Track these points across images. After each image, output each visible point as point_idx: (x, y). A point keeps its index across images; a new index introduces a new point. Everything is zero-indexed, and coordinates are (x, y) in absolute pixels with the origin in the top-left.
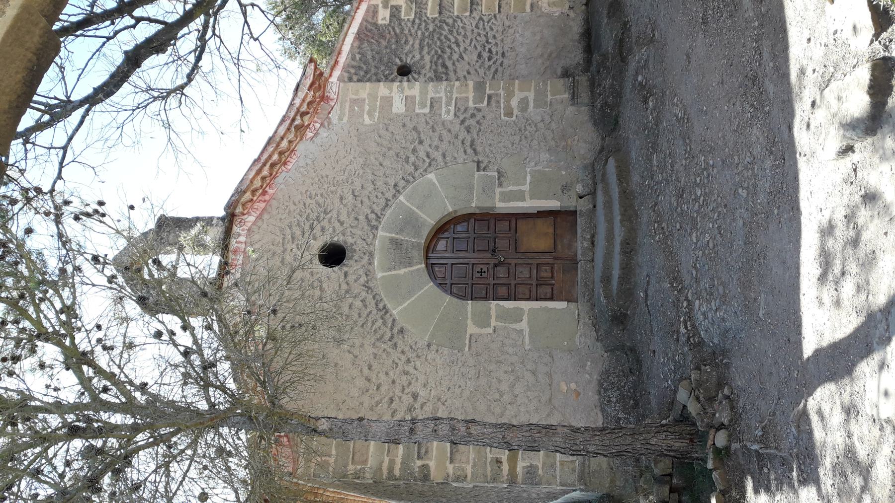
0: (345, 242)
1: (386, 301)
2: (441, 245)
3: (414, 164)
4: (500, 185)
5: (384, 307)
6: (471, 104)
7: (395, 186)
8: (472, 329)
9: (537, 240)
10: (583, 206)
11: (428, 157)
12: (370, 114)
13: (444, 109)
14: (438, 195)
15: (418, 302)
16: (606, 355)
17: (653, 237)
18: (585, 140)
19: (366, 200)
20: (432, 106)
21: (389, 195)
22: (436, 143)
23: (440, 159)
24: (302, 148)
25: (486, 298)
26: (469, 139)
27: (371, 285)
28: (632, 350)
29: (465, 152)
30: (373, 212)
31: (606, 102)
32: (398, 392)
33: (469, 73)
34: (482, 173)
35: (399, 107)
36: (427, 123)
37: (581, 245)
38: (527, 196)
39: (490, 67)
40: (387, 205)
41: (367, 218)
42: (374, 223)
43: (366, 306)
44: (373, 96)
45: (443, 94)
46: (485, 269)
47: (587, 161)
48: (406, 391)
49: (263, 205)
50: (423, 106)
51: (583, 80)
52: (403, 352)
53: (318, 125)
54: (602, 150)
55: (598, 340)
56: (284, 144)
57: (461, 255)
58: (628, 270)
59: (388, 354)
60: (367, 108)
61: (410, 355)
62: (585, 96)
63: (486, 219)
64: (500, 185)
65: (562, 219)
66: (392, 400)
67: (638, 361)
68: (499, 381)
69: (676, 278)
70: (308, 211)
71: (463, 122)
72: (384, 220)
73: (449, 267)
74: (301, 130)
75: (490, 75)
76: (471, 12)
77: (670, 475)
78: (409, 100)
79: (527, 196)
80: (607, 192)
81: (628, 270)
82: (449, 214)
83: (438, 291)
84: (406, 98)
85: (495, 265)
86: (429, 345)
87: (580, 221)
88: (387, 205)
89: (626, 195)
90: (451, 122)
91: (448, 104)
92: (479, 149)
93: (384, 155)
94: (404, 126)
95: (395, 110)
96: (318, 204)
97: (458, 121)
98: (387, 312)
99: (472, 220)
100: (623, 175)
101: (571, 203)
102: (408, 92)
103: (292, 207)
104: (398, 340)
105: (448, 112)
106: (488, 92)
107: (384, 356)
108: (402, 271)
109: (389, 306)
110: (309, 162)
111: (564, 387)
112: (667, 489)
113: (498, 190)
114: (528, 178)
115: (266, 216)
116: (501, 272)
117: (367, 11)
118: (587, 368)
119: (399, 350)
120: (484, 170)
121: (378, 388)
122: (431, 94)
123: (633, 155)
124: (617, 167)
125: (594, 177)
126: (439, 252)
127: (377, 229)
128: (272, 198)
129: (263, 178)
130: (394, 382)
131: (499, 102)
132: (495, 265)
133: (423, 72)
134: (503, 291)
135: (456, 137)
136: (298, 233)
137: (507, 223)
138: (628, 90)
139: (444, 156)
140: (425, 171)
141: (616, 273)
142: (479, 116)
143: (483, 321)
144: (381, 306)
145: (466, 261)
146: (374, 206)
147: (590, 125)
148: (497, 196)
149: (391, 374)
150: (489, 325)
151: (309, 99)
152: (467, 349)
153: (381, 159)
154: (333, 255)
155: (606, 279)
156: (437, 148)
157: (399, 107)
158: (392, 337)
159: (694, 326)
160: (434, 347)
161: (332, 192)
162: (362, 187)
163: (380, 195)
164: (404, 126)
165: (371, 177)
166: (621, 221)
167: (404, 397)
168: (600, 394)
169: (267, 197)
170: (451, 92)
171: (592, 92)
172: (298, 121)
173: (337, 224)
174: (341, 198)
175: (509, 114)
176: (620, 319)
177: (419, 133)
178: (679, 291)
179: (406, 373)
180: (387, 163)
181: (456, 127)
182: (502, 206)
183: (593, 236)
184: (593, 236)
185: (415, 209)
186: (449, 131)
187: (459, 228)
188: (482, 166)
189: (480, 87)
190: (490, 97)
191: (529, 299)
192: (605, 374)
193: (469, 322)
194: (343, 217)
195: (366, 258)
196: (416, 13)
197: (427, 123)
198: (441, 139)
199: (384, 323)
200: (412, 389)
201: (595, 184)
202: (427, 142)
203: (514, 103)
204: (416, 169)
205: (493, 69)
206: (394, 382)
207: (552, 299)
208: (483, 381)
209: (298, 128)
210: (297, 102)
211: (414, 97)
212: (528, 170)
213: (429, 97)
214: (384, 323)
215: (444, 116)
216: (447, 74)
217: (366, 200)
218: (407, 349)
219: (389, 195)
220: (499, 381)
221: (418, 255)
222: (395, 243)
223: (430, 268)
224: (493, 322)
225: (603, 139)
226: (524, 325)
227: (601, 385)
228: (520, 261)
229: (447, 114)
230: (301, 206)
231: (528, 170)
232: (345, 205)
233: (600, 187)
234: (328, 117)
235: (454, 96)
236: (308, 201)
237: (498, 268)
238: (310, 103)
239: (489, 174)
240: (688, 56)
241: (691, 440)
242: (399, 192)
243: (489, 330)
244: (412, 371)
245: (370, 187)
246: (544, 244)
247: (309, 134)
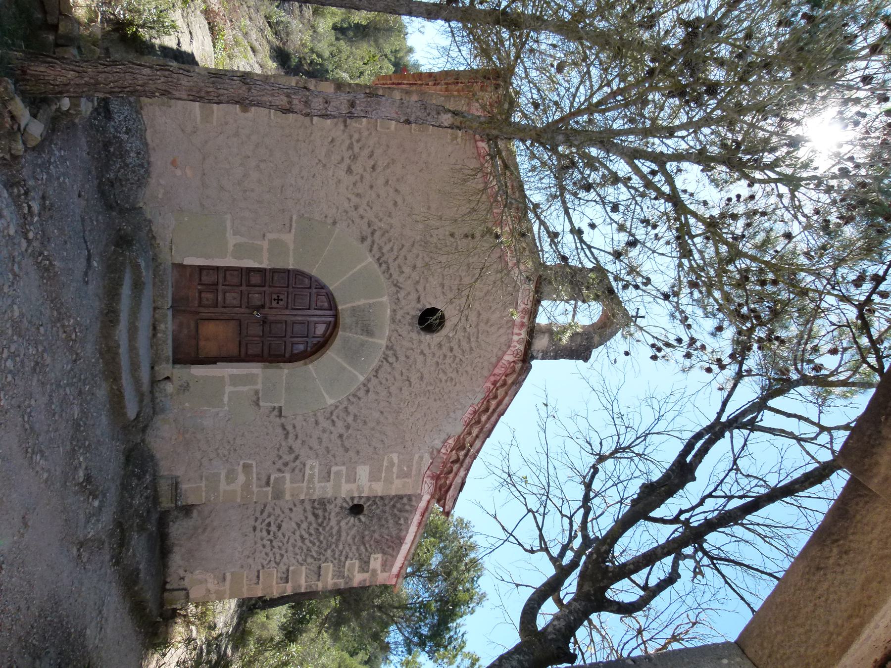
0: (418, 333)
1: (379, 271)
2: (320, 329)
3: (348, 413)
4: (257, 392)
5: (380, 265)
6: (288, 476)
7: (368, 391)
8: (288, 238)
9: (216, 334)
10: (165, 369)
11: (333, 421)
12: (392, 464)
13: (316, 470)
14: (323, 382)
15: (345, 270)
16: (141, 205)
17: (78, 324)
18: (163, 440)
19: (398, 376)
20: (329, 473)
21: (374, 381)
22: (326, 435)
23: (321, 419)
24: (457, 428)
25: (274, 271)
26: (291, 440)
27: (394, 289)
28: (110, 207)
29: (294, 427)
30: (391, 364)
31: (139, 479)
32: (367, 176)
33: (291, 510)
34: (276, 405)
35: (363, 472)
36: (334, 456)
37: (168, 326)
38: (227, 380)
39: (269, 516)
40: (377, 371)
41: (397, 358)
42: (390, 353)
43: (400, 267)
44: (389, 481)
45: (317, 485)
46: (274, 303)
47: (161, 417)
48: (358, 177)
49: (497, 371)
50: (338, 473)
51: (166, 503)
52: (362, 217)
53: (443, 451)
54: (144, 430)
55: (150, 221)
56: (475, 431)
57: (300, 319)
58: (112, 293)
59: (377, 217)
60: (395, 470)
61: (354, 214)
62: (164, 487)
63: (273, 356)
64: (257, 392)
65: (189, 355)
66: (373, 167)
67: (103, 194)
68: (259, 181)
69: (46, 271)
70: (454, 365)
71: (297, 458)
72: (380, 355)
73: (313, 305)
74: (460, 446)
75: (268, 509)
76: (288, 570)
77: (57, 45)
79: (227, 380)
80: (137, 382)
81: (112, 293)
82: (311, 362)
83: (325, 280)
85: (263, 306)
86: (334, 223)
87: (168, 351)
88: (377, 371)
89: (112, 375)
90: (308, 457)
91: (312, 476)
92: (279, 430)
93: (378, 423)
94: (358, 452)
95: (366, 469)
96: (444, 372)
97: (301, 459)
98: (378, 259)
99: (287, 355)
100: (117, 400)
101: (181, 373)
102: (353, 486)
103: (469, 369)
104: (367, 231)
105: (312, 468)
106: (269, 489)
107: (381, 214)
108: (362, 302)
109: (376, 266)
110: (452, 414)
111: (189, 172)
112: (62, 29)
113: (259, 386)
114: (226, 399)
115: (494, 360)
116: (256, 299)
117: (392, 566)
118: (162, 191)
119: (366, 220)
120: (274, 408)
121: (387, 182)
122: (330, 485)
123: (104, 420)
124: (123, 407)
125: (153, 400)
126: (324, 322)
127: (387, 347)
128: (487, 378)
129: (495, 397)
130: (371, 187)
131: (258, 479)
132: (263, 306)
133: (337, 509)
134: (255, 279)
136: (464, 344)
137: (250, 352)
139: (317, 423)
140: (337, 407)
141: (126, 291)
142: (279, 464)
143: (276, 244)
144: (384, 266)
145: (295, 312)
146: (389, 370)
147: (158, 456)
148: (260, 381)
149: (374, 196)
150: (270, 241)
151: (451, 476)
152: (295, 217)
153: (382, 419)
154: (430, 320)
155: (138, 286)
156: (324, 431)
157: (363, 472)
158: (373, 234)
159: (19, 207)
160: (330, 221)
161: (431, 384)
162: (401, 389)
163: (384, 381)
164: (358, 452)
165: (393, 400)
166: (118, 346)
167: (361, 171)
168: (149, 163)
169: (492, 379)
170: (309, 488)
171: (156, 490)
172: (462, 454)
173: (426, 351)
174: (422, 378)
175: (246, 467)
176: (123, 241)
177: (343, 445)
178: (41, 254)
179: (358, 195)
180: (376, 415)
181: (303, 452)
182: (255, 369)
183: (154, 335)
184: (154, 335)
185: (350, 368)
186: (311, 448)
187: (301, 347)
188: (276, 412)
189: (278, 495)
190: (268, 484)
191: (227, 269)
192: (142, 182)
193: (292, 247)
194: (420, 359)
195: (398, 317)
196: (344, 566)
197: (334, 456)
199: (380, 248)
200: (353, 179)
201: (152, 392)
202: (334, 437)
203: (241, 478)
204: (346, 408)
205: (265, 514)
206: (371, 187)
207: (201, 268)
209: (462, 447)
210: (462, 473)
211: (348, 481)
212: (226, 408)
213: (332, 482)
214: (380, 248)
215: (316, 463)
216: (314, 508)
217: (398, 376)
218: (357, 220)
219: (374, 381)
220: (259, 181)
221: (345, 319)
222: (368, 331)
223: (332, 305)
224: (265, 245)
225: (143, 441)
226: (232, 240)
227: (148, 172)
228: (236, 310)
229: (313, 466)
230: (460, 370)
231: (226, 408)
232: (419, 371)
233: (146, 387)
234: (433, 459)
235: (305, 484)
236: (454, 375)
237: (259, 303)
238: (450, 472)
239: (268, 404)
240: (26, 525)
241: (24, 72)
242: (364, 385)
243: (270, 236)
244: (353, 197)
245: (393, 389)
246: (210, 329)
247: (451, 441)
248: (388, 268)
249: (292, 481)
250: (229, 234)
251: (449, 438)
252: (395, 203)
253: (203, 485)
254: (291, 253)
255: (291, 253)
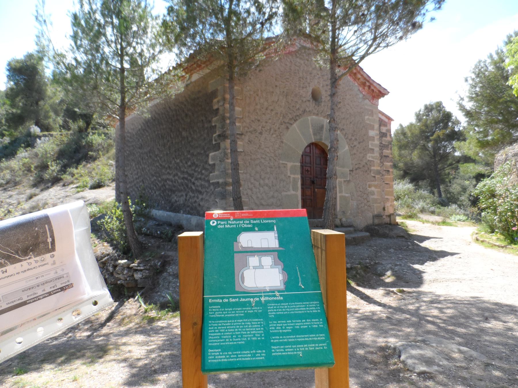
4: (345, 181)
5: (297, 120)
7: (343, 129)
8: (289, 165)
12: (368, 119)
26: (361, 166)
29: (356, 164)
38: (341, 194)
45: (375, 155)
52: (279, 128)
66: (259, 121)
68: (269, 179)
74: (364, 84)
76: (385, 171)
84: (374, 137)
91: (372, 157)
104: (283, 126)
106: (377, 176)
108: (311, 130)
109: (297, 122)
117: (385, 122)
120: (350, 173)
135: (361, 160)
138: (380, 242)
144: (297, 118)
147: (366, 224)
148: (340, 180)
150: (291, 174)
151: (375, 90)
158: (285, 123)
172: (368, 84)
188: (351, 172)
190: (374, 177)
195: (316, 112)
196: (384, 145)
198: (360, 153)
203: (373, 189)
208: (268, 170)
210: (375, 84)
213: (374, 148)
224: (292, 176)
226: (293, 192)
234: (367, 98)
238: (373, 90)
243: (289, 174)
247: (361, 89)
248: (298, 116)
249: (374, 166)
250: (289, 193)
251: (359, 90)
252: (272, 110)
253: (375, 205)
254: (295, 164)
255: (295, 164)
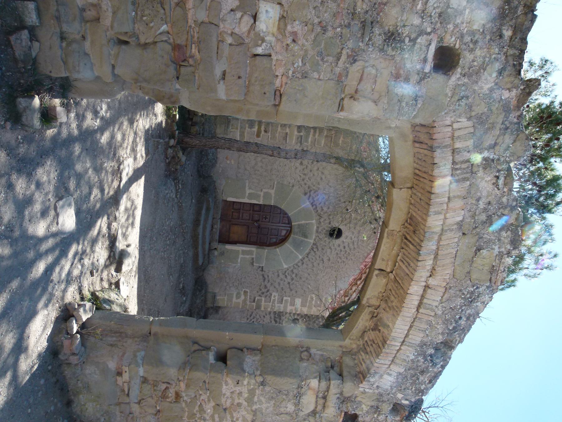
0: (329, 238)
1: (312, 208)
2: (284, 233)
3: (293, 273)
4: (253, 259)
5: (313, 206)
6: (263, 299)
7: (303, 263)
8: (272, 192)
9: (238, 231)
10: (215, 245)
11: (286, 276)
13: (276, 298)
14: (283, 258)
16: (212, 175)
17: (187, 226)
18: (211, 275)
19: (318, 258)
20: (282, 300)
21: (306, 259)
22: (282, 282)
23: (281, 274)
24: (347, 286)
25: (265, 205)
26: (266, 282)
27: (318, 217)
28: (200, 176)
30: (315, 252)
31: (200, 291)
32: (309, 166)
33: (264, 316)
34: (261, 265)
35: (298, 301)
36: (285, 292)
37: (218, 226)
38: (241, 252)
39: (254, 318)
40: (308, 255)
41: (318, 249)
42: (315, 246)
43: (322, 207)
44: (310, 307)
45: (277, 305)
46: (264, 219)
47: (211, 265)
48: (305, 166)
49: (367, 260)
50: (286, 301)
51: (209, 305)
52: (305, 184)
53: (338, 296)
54: (204, 270)
55: (215, 182)
56: (354, 289)
57: (274, 227)
58: (198, 213)
59: (312, 184)
60: (313, 302)
61: (302, 183)
62: (209, 296)
63: (261, 243)
64: (253, 259)
65: (225, 239)
67: (198, 171)
68: (262, 167)
69: (180, 207)
70: (345, 255)
71: (268, 291)
72: (310, 247)
73: (281, 222)
75: (254, 315)
77: (192, 125)
78: (293, 304)
79: (241, 252)
80: (204, 249)
81: (198, 213)
82: (278, 247)
83: (288, 212)
85: (259, 220)
86: (293, 186)
87: (217, 237)
88: (308, 255)
89: (195, 247)
90: (273, 291)
91: (274, 300)
92: (261, 277)
93: (307, 279)
94: (296, 292)
95: (300, 300)
96: (340, 258)
97: (270, 292)
98: (312, 203)
99: (268, 243)
100: (196, 256)
101: (220, 247)
102: (293, 308)
103: (353, 258)
105: (274, 296)
106: (255, 304)
107: (314, 183)
108: (303, 222)
109: (310, 206)
110: (343, 279)
111: (233, 162)
112: (194, 120)
113: (254, 256)
114: (239, 261)
115: (366, 255)
116: (256, 217)
118: (221, 169)
119: (307, 185)
121: (318, 169)
122: (282, 306)
123: (190, 264)
124: (198, 260)
125: (209, 257)
126: (285, 230)
127: (313, 244)
128: (362, 263)
129: (365, 273)
130: (311, 171)
131: (250, 298)
132: (259, 220)
133: (286, 320)
134: (256, 208)
135: (272, 284)
136: (351, 245)
137: (252, 240)
139: (278, 276)
140: (288, 269)
141: (204, 212)
142: (260, 293)
143: (267, 195)
144: (314, 207)
145: (272, 224)
146: (314, 254)
148: (255, 253)
149: (312, 175)
152: (276, 183)
153: (309, 277)
154: (336, 233)
155: (208, 209)
156: (281, 280)
157: (298, 301)
158: (310, 191)
159: (176, 187)
160: (291, 185)
161: (333, 263)
162: (319, 264)
163: (311, 260)
164: (296, 292)
165: (314, 269)
166: (199, 235)
167: (306, 164)
168: (217, 158)
169: (364, 264)
170: (272, 306)
171: (206, 298)
173: (332, 247)
174: (329, 260)
175: (245, 292)
176: (204, 190)
177: (289, 287)
178: (179, 202)
179: (304, 174)
180: (306, 275)
181: (271, 289)
182: (253, 249)
183: (212, 230)
184: (212, 230)
185: (295, 252)
186: (275, 287)
187: (274, 240)
188: (260, 269)
189: (258, 307)
190: (254, 301)
191: (244, 203)
192: (213, 165)
193: (273, 195)
194: (329, 250)
195: (320, 230)
197: (285, 292)
199: (313, 198)
200: (302, 167)
201: (208, 254)
202: (286, 283)
203: (243, 297)
204: (292, 270)
205: (252, 317)
206: (311, 171)
207: (234, 202)
209: (347, 296)
211: (291, 305)
212: (239, 264)
214: (313, 198)
215: (277, 295)
216: (275, 317)
217: (318, 258)
218: (303, 185)
219: (306, 259)
220: (262, 167)
221: (295, 230)
222: (305, 236)
223: (290, 222)
224: (262, 194)
225: (203, 275)
226: (248, 191)
227: (216, 162)
228: (247, 221)
229: (275, 295)
230: (349, 258)
231: (239, 264)
232: (328, 256)
233: (207, 252)
235: (271, 304)
236: (345, 260)
237: (257, 219)
239: (258, 265)
240: (166, 301)
241: (183, 141)
242: (302, 260)
243: (264, 190)
244: (302, 175)
245: (315, 264)
246: (235, 229)
248: (316, 207)
249: (265, 302)
250: (247, 188)
251: (341, 290)
252: (321, 179)
253: (226, 298)
254: (273, 199)
255: (273, 199)
